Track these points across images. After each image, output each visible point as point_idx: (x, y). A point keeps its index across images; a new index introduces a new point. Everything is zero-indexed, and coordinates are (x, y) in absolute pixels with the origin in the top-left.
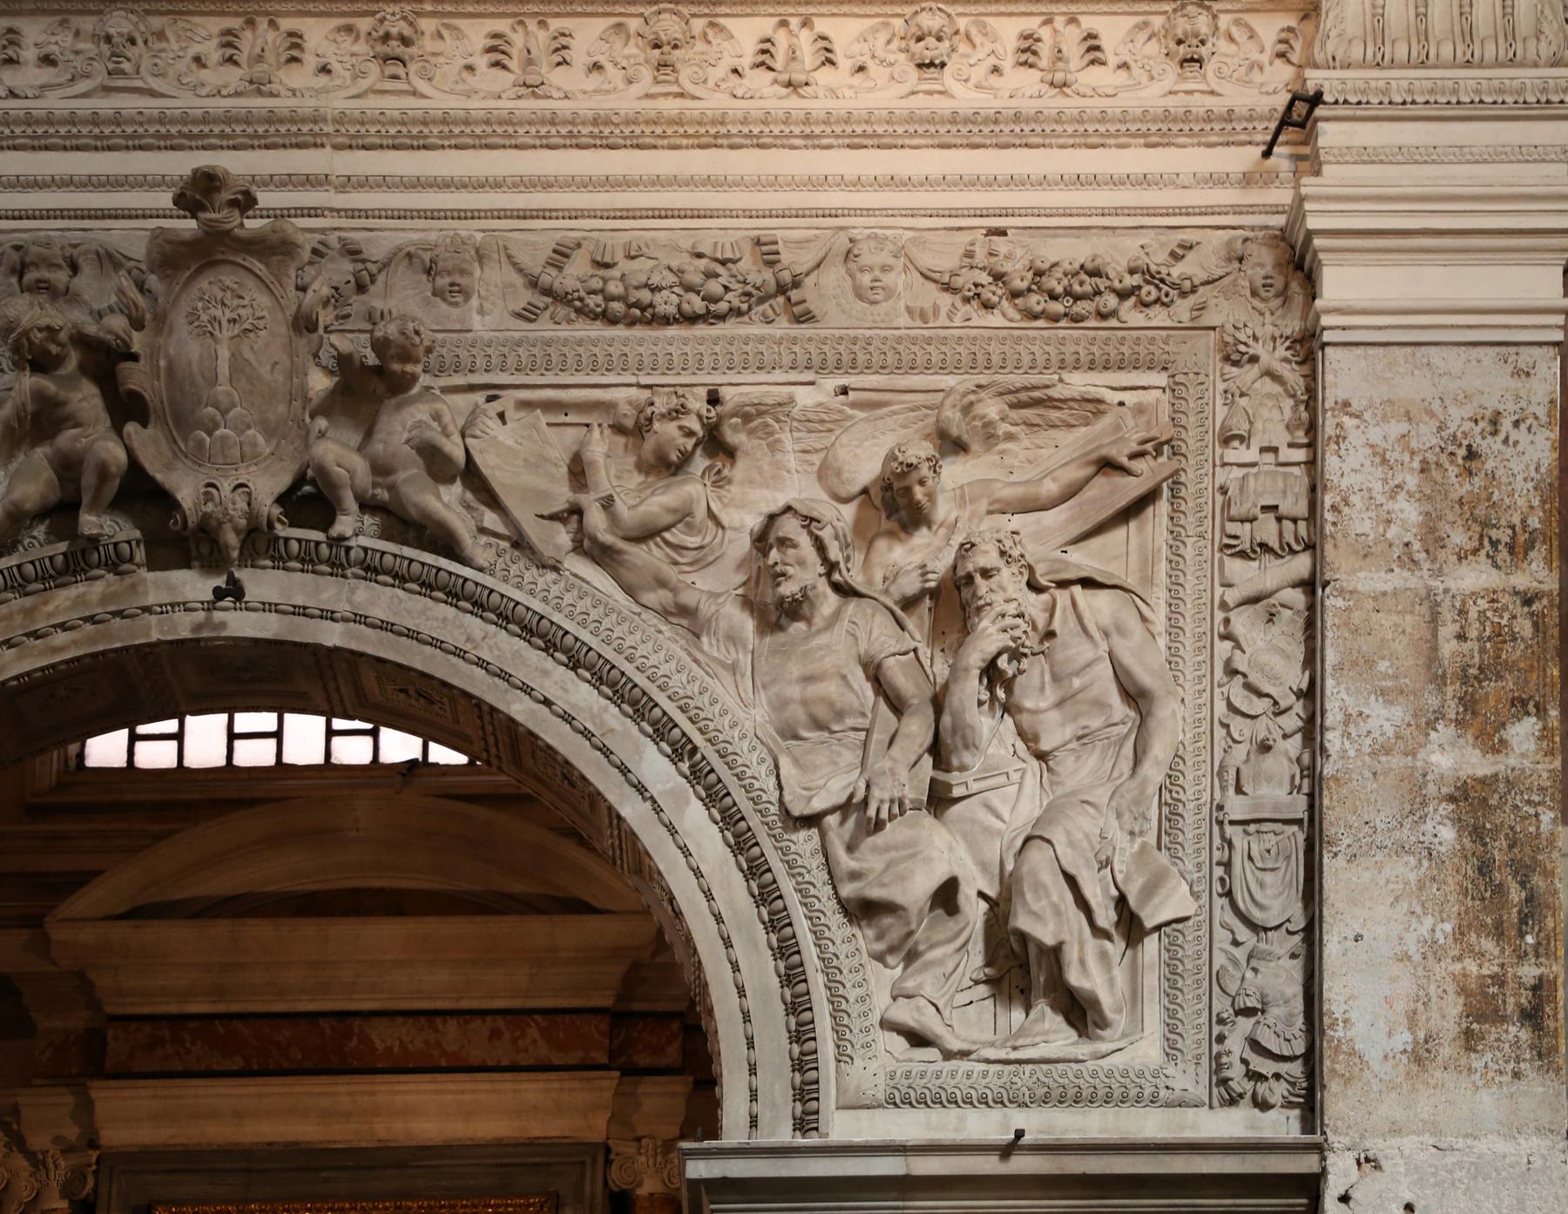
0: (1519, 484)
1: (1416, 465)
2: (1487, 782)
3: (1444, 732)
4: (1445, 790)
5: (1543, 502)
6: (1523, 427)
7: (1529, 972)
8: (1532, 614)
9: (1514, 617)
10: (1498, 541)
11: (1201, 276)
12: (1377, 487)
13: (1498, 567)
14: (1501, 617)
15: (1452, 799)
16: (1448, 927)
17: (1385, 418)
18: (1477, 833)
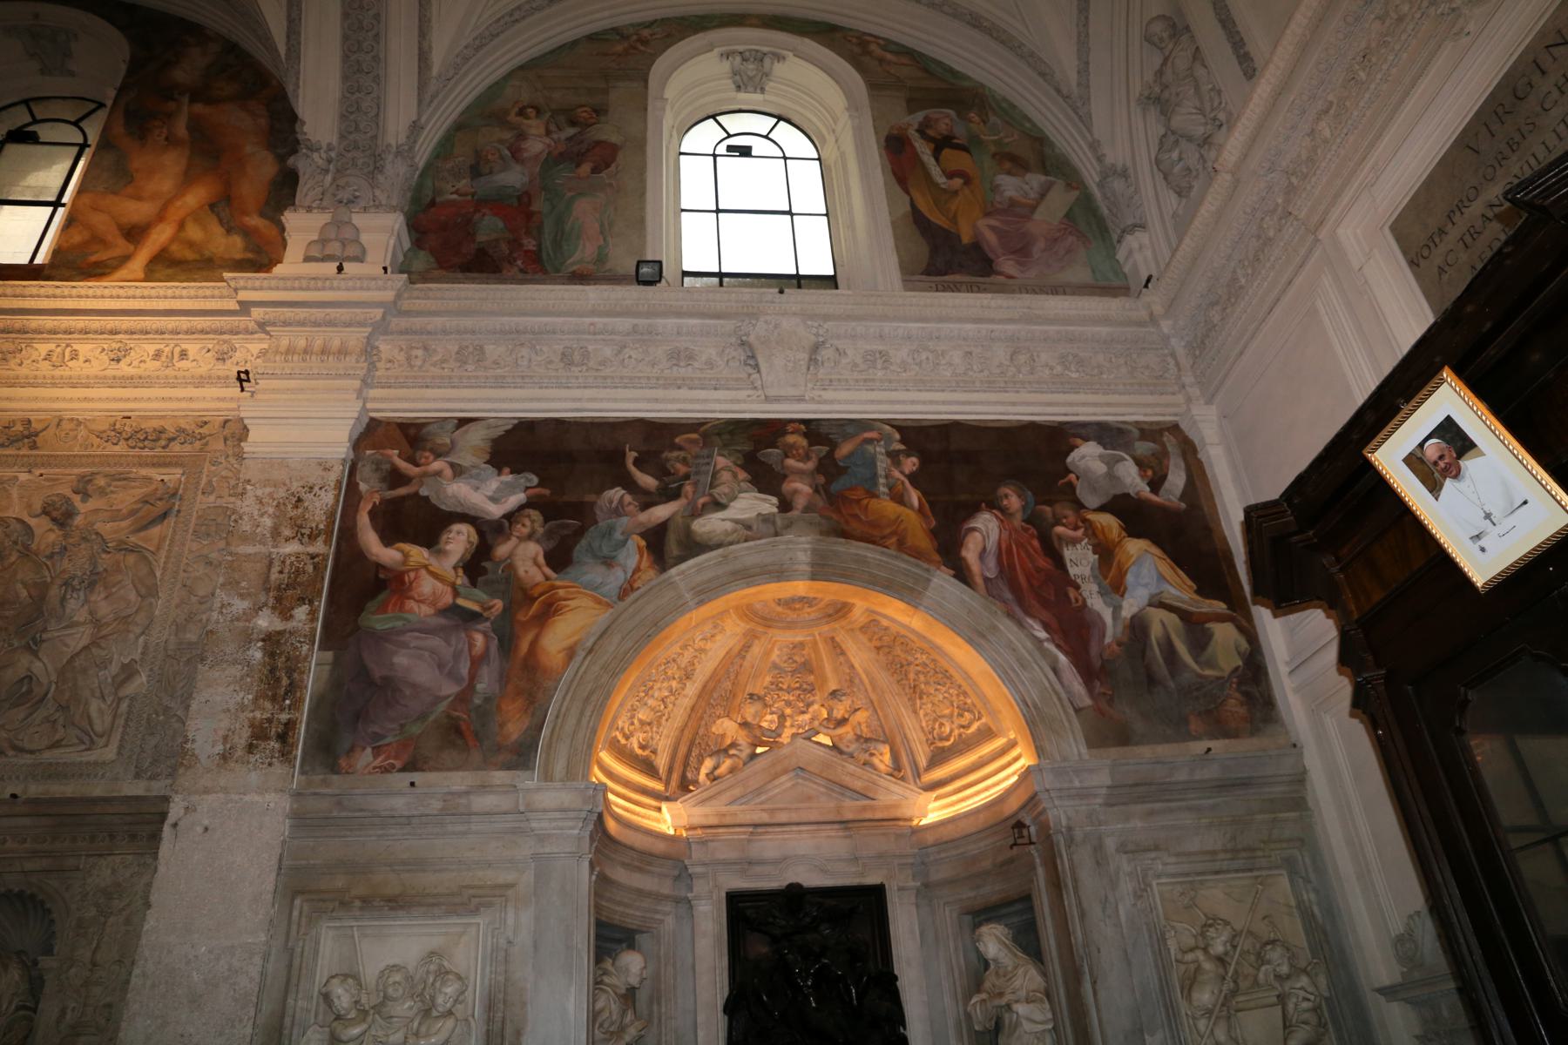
0: (318, 511)
1: (274, 504)
2: (280, 633)
3: (266, 611)
4: (261, 636)
7: (284, 717)
11: (208, 433)
12: (256, 513)
15: (263, 640)
16: (250, 697)
17: (265, 486)
18: (272, 655)
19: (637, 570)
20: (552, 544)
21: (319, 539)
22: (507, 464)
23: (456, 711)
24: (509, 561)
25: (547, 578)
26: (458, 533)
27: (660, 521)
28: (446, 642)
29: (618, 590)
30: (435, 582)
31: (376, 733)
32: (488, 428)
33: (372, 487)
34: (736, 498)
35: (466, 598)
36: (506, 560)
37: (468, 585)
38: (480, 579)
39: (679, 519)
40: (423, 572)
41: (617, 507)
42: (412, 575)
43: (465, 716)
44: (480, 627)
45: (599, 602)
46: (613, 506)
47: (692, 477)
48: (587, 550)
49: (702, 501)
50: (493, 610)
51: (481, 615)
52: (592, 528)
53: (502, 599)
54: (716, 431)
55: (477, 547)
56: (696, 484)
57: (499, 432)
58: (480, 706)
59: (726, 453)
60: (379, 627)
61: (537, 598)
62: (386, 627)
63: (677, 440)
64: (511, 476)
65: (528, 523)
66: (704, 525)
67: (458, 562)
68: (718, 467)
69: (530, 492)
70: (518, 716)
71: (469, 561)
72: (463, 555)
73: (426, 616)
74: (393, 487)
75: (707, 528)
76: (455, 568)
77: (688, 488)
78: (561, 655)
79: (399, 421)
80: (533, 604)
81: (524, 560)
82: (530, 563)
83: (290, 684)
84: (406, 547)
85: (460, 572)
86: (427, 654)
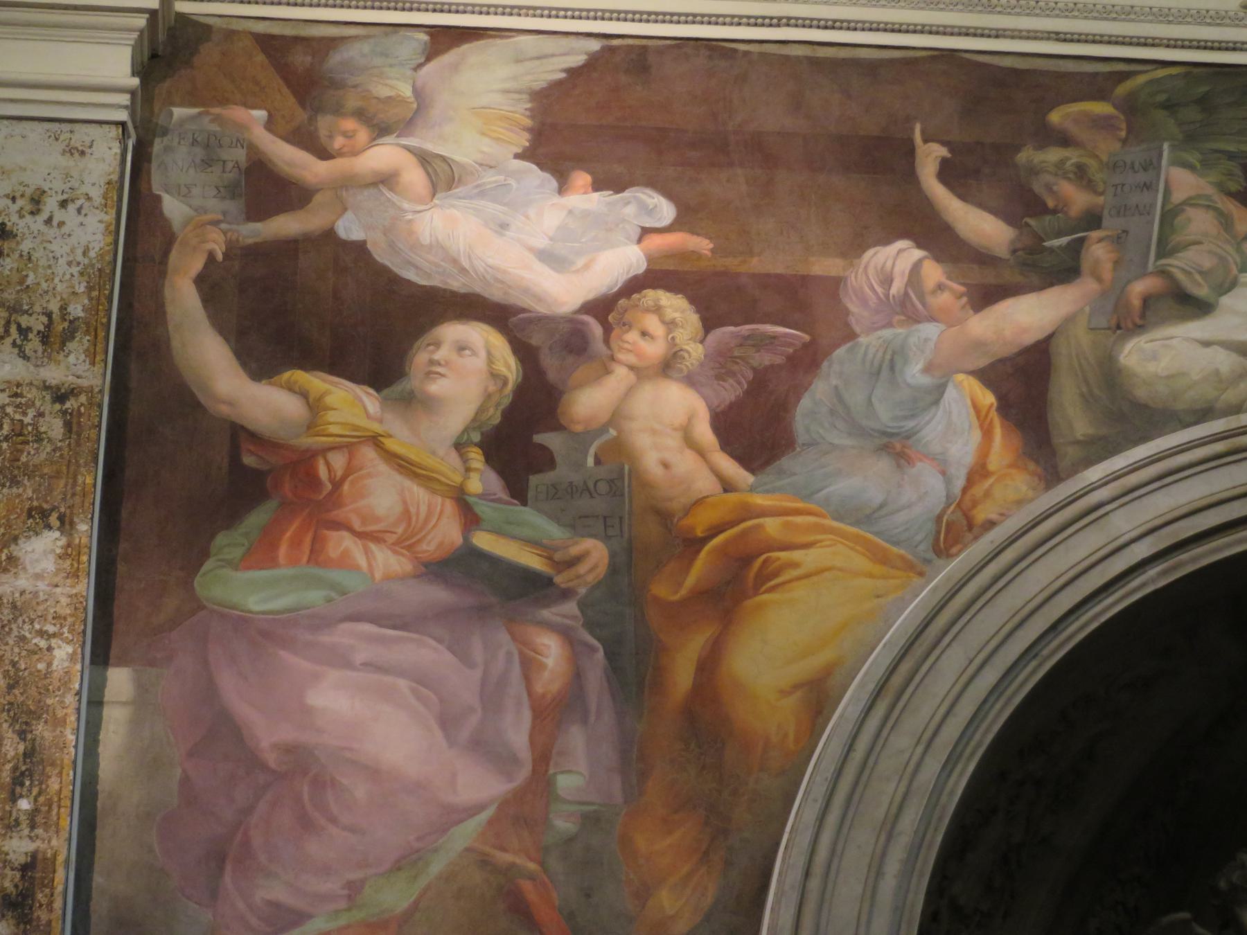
0: (61, 267)
5: (90, 289)
6: (72, 208)
8: (65, 412)
9: (41, 415)
10: (29, 329)
13: (25, 357)
14: (25, 414)
19: (978, 472)
20: (730, 392)
21: (71, 346)
22: (580, 162)
23: (504, 849)
24: (613, 432)
25: (728, 486)
27: (1029, 339)
29: (930, 526)
31: (275, 905)
32: (518, 61)
33: (200, 210)
34: (1233, 284)
35: (499, 532)
36: (603, 429)
37: (505, 496)
38: (534, 480)
39: (1081, 336)
40: (368, 454)
41: (906, 294)
42: (338, 461)
43: (532, 866)
44: (546, 614)
45: (881, 558)
47: (1105, 223)
48: (832, 412)
49: (1139, 288)
50: (582, 568)
51: (549, 582)
52: (840, 352)
53: (606, 538)
54: (1161, 98)
55: (521, 391)
56: (1119, 240)
57: (551, 71)
58: (571, 840)
59: (1193, 158)
61: (704, 541)
63: (1055, 117)
64: (596, 195)
65: (653, 323)
66: (1155, 357)
67: (466, 430)
68: (1178, 197)
69: (656, 242)
70: (686, 869)
71: (498, 428)
72: (481, 410)
73: (388, 578)
74: (258, 210)
75: (1163, 366)
76: (459, 446)
77: (1098, 251)
78: (791, 702)
79: (260, 28)
80: (698, 551)
81: (654, 432)
82: (673, 442)
83: (27, 755)
84: (316, 382)
85: (476, 458)
86: (403, 684)
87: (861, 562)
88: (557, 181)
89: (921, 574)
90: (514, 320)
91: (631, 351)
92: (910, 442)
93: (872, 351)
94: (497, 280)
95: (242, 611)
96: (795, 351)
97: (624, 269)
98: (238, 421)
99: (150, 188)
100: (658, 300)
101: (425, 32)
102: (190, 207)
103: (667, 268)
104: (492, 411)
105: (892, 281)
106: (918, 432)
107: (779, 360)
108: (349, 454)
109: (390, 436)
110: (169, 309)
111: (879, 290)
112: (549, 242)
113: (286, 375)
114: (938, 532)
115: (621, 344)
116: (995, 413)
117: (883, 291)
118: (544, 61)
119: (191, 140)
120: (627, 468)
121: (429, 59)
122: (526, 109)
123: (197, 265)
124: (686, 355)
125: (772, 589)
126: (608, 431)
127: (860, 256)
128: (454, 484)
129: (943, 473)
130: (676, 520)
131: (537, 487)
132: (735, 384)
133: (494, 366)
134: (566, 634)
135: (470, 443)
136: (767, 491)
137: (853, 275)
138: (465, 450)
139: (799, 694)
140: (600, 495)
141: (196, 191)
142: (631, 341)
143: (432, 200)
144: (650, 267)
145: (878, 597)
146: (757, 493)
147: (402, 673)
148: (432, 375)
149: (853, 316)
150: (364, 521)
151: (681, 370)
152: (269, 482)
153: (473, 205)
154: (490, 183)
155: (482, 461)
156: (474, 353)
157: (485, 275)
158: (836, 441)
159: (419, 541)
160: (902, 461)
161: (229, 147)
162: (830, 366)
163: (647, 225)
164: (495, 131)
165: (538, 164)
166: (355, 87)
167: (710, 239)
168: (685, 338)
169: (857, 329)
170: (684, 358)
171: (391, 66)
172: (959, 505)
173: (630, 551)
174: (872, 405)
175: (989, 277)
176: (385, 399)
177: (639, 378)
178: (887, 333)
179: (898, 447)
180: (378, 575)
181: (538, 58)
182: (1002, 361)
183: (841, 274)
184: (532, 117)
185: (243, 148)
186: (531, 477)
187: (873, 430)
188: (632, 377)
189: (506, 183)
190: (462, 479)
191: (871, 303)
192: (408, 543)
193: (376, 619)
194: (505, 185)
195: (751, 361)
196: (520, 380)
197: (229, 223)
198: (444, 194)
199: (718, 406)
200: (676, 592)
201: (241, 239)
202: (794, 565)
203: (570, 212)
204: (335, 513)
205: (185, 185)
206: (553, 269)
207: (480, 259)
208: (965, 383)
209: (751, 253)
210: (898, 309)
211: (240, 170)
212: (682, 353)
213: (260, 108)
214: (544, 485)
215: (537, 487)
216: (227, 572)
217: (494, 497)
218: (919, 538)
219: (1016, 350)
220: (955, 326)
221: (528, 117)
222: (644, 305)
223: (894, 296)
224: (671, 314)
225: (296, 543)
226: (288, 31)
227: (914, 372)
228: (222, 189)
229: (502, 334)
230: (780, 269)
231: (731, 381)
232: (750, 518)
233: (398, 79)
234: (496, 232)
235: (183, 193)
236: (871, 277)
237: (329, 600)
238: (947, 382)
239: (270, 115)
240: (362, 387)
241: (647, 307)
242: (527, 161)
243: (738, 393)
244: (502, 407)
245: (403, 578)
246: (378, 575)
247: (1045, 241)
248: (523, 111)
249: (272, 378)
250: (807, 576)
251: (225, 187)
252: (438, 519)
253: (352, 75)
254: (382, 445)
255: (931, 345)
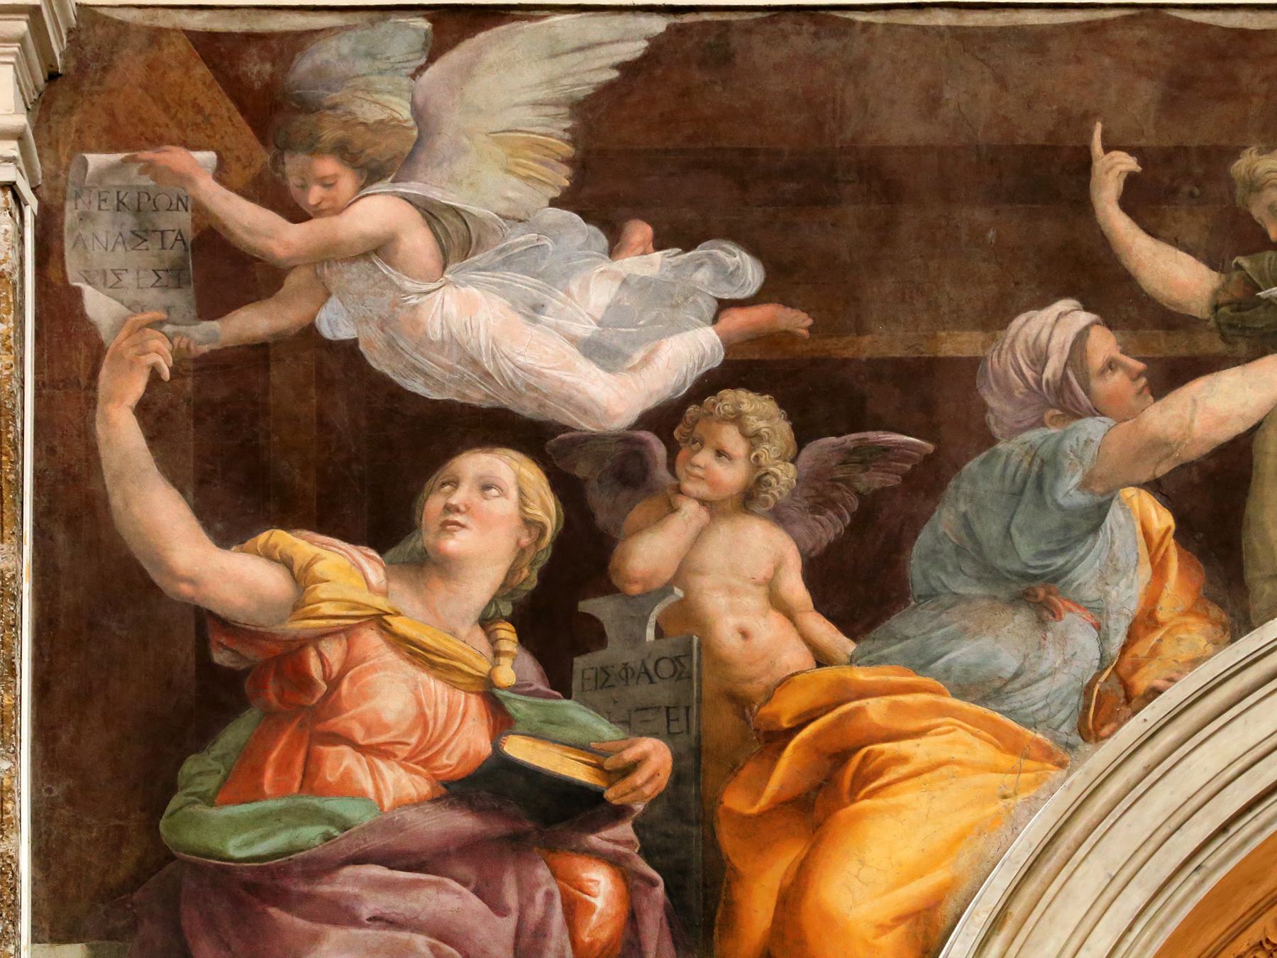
19: (1145, 622)
20: (829, 528)
24: (679, 593)
25: (822, 659)
26: (486, 487)
27: (1224, 434)
28: (478, 893)
29: (1075, 699)
30: (423, 676)
32: (554, 56)
35: (536, 735)
36: (666, 590)
37: (544, 688)
38: (580, 663)
40: (371, 639)
41: (1065, 377)
42: (334, 651)
44: (594, 840)
45: (1013, 746)
46: (1048, 374)
48: (959, 550)
50: (639, 778)
52: (973, 465)
53: (669, 736)
55: (560, 542)
60: (236, 848)
62: (261, 849)
64: (658, 256)
65: (731, 438)
67: (494, 600)
69: (737, 320)
71: (534, 595)
72: (512, 572)
73: (400, 804)
76: (486, 622)
82: (754, 601)
85: (507, 636)
87: (984, 752)
88: (607, 238)
89: (1061, 765)
90: (552, 442)
91: (703, 479)
92: (1058, 586)
93: (1015, 460)
94: (529, 387)
95: (221, 859)
96: (914, 467)
97: (694, 363)
98: (205, 605)
99: (64, 278)
100: (739, 403)
101: (425, 16)
102: (122, 302)
103: (751, 357)
104: (526, 572)
105: (1047, 359)
106: (1067, 573)
107: (893, 481)
108: (347, 640)
109: (398, 614)
110: (104, 452)
111: (1028, 373)
112: (597, 328)
113: (263, 537)
114: (1087, 707)
115: (689, 468)
116: (1172, 541)
117: (1035, 374)
118: (589, 53)
119: (116, 202)
120: (695, 639)
121: (432, 59)
122: (565, 130)
123: (137, 387)
124: (773, 480)
125: (870, 795)
126: (672, 592)
127: (1004, 326)
128: (481, 675)
129: (1098, 627)
130: (756, 707)
131: (583, 672)
132: (834, 517)
133: (528, 510)
134: (615, 862)
135: (499, 617)
136: (870, 663)
137: (995, 353)
138: (492, 627)
139: (902, 928)
140: (663, 679)
141: (128, 279)
142: (702, 465)
143: (442, 276)
144: (729, 357)
145: (1005, 797)
146: (859, 665)
147: (418, 928)
148: (448, 527)
149: (992, 413)
150: (369, 731)
151: (767, 501)
152: (248, 687)
153: (495, 280)
154: (518, 245)
155: (514, 642)
156: (503, 493)
157: (515, 381)
158: (961, 591)
159: (438, 753)
160: (1046, 613)
161: (168, 210)
162: (957, 487)
163: (726, 297)
164: (524, 166)
165: (581, 214)
166: (334, 107)
167: (808, 312)
168: (772, 456)
169: (996, 431)
170: (770, 485)
171: (381, 72)
172: (1115, 669)
173: (697, 751)
174: (1011, 538)
175: (1176, 346)
176: (390, 563)
177: (712, 516)
178: (1034, 436)
179: (1042, 593)
180: (387, 803)
181: (580, 49)
182: (1185, 467)
183: (980, 353)
184: (573, 142)
185: (187, 210)
186: (576, 660)
187: (1008, 572)
188: (704, 515)
189: (539, 243)
190: (491, 667)
191: (1017, 393)
192: (423, 757)
193: (389, 859)
194: (538, 246)
195: (858, 485)
196: (561, 527)
197: (174, 324)
198: (457, 264)
199: (813, 549)
200: (753, 803)
201: (192, 346)
202: (902, 760)
203: (625, 282)
204: (333, 721)
205: (113, 270)
206: (603, 367)
207: (506, 357)
208: (1135, 501)
209: (861, 330)
210: (1052, 400)
211: (184, 243)
212: (768, 477)
213: (207, 149)
214: (592, 668)
215: (583, 672)
216: (201, 809)
217: (527, 689)
218: (1061, 716)
219: (1207, 450)
220: (1128, 420)
221: (568, 141)
222: (720, 413)
223: (1047, 382)
224: (755, 424)
225: (284, 766)
226: (236, 25)
227: (1069, 488)
228: (160, 273)
229: (538, 464)
230: (899, 352)
231: (830, 513)
232: (849, 701)
233: (389, 92)
234: (528, 317)
235: (109, 281)
236: (1019, 355)
237: (328, 838)
238: (1111, 500)
239: (220, 159)
240: (360, 547)
241: (725, 415)
242: (567, 209)
243: (838, 530)
244: (539, 566)
245: (417, 803)
246: (387, 803)
247: (1260, 290)
248: (561, 133)
249: (243, 542)
250: (917, 774)
251: (167, 271)
252: (461, 723)
253: (329, 89)
254: (388, 627)
255: (1093, 449)
